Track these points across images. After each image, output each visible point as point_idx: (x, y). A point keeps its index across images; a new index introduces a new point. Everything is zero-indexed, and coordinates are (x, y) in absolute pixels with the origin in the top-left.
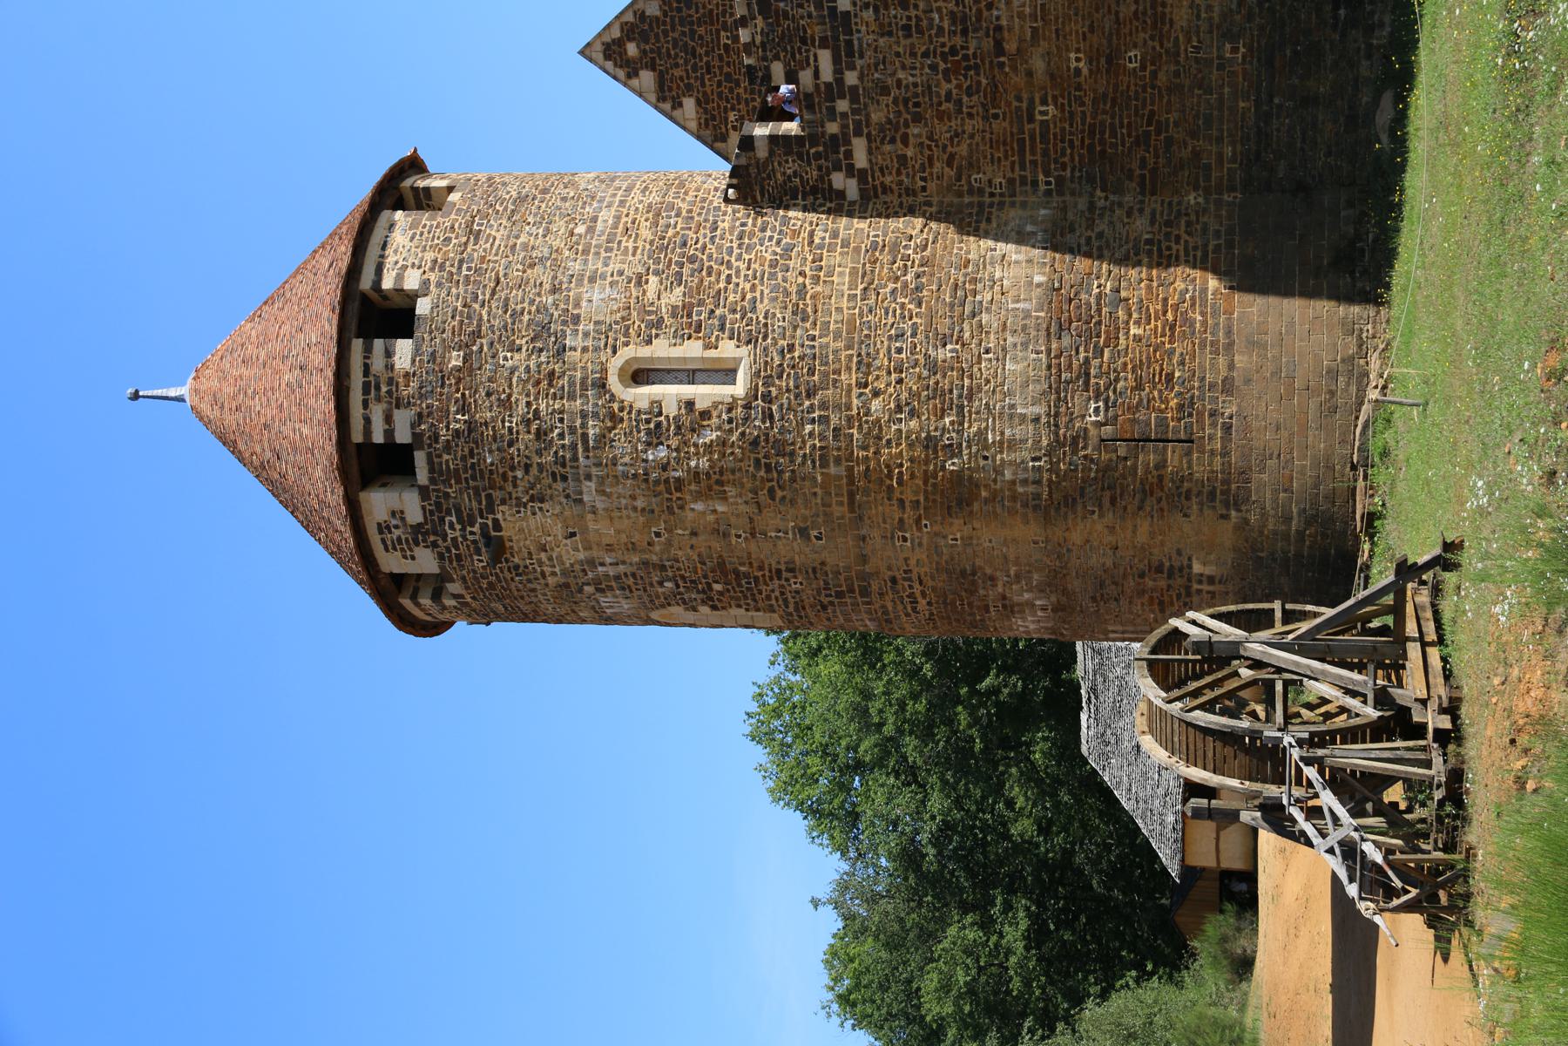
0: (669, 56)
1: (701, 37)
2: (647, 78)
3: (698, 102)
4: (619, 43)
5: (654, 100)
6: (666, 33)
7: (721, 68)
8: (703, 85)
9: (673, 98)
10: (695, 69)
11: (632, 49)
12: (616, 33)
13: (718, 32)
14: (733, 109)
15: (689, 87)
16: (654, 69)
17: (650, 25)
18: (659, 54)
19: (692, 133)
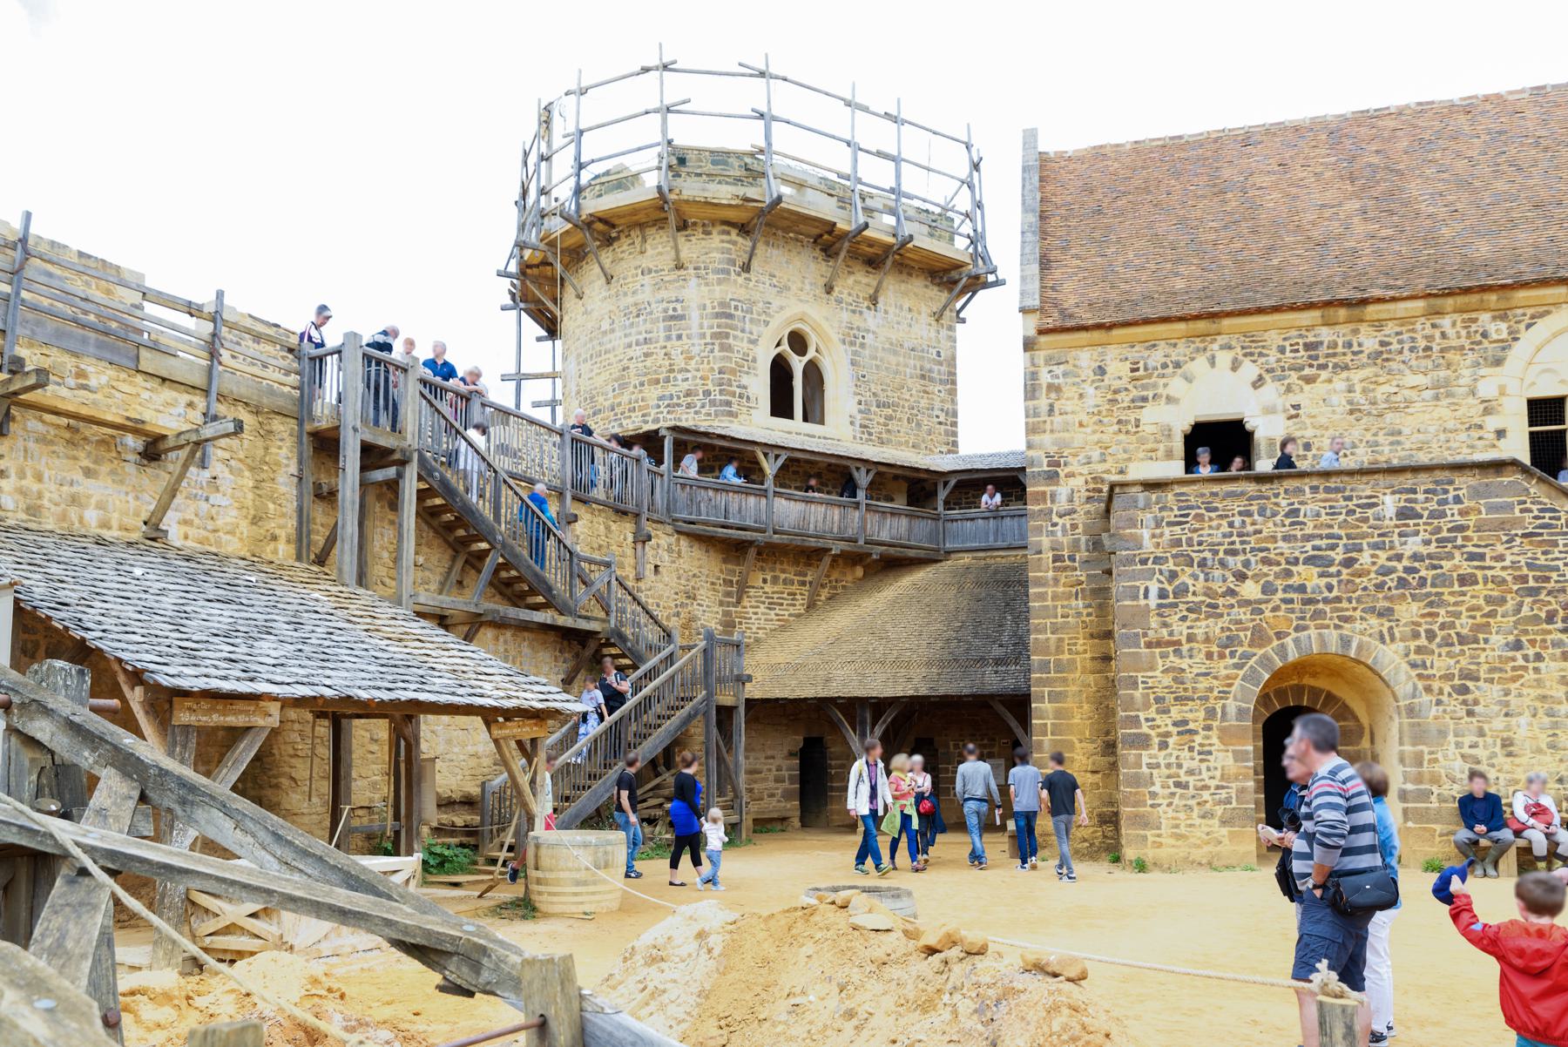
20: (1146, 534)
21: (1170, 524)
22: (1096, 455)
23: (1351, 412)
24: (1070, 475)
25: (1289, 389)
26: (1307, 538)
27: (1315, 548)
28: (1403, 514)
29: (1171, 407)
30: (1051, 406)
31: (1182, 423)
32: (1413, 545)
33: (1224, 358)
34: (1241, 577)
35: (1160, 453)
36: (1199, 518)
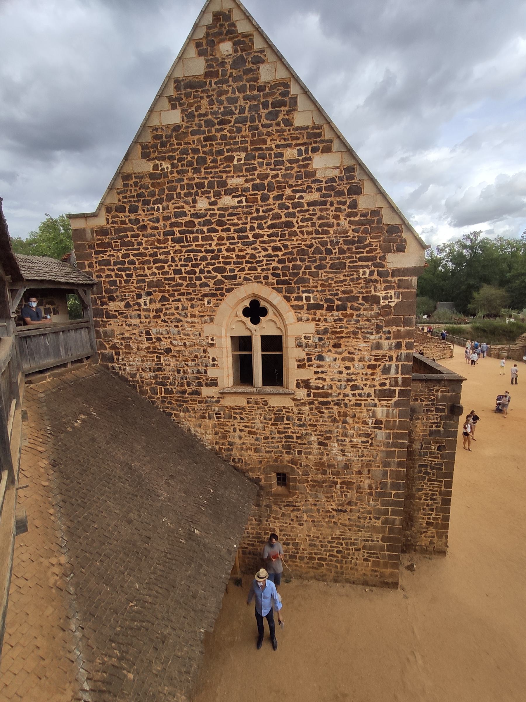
0: (220, 94)
1: (239, 130)
2: (197, 67)
3: (177, 128)
4: (231, 33)
5: (179, 74)
6: (242, 90)
7: (210, 153)
8: (193, 133)
9: (179, 99)
10: (209, 123)
11: (226, 48)
12: (242, 27)
13: (245, 150)
14: (173, 166)
15: (190, 116)
16: (207, 75)
17: (250, 70)
18: (222, 82)
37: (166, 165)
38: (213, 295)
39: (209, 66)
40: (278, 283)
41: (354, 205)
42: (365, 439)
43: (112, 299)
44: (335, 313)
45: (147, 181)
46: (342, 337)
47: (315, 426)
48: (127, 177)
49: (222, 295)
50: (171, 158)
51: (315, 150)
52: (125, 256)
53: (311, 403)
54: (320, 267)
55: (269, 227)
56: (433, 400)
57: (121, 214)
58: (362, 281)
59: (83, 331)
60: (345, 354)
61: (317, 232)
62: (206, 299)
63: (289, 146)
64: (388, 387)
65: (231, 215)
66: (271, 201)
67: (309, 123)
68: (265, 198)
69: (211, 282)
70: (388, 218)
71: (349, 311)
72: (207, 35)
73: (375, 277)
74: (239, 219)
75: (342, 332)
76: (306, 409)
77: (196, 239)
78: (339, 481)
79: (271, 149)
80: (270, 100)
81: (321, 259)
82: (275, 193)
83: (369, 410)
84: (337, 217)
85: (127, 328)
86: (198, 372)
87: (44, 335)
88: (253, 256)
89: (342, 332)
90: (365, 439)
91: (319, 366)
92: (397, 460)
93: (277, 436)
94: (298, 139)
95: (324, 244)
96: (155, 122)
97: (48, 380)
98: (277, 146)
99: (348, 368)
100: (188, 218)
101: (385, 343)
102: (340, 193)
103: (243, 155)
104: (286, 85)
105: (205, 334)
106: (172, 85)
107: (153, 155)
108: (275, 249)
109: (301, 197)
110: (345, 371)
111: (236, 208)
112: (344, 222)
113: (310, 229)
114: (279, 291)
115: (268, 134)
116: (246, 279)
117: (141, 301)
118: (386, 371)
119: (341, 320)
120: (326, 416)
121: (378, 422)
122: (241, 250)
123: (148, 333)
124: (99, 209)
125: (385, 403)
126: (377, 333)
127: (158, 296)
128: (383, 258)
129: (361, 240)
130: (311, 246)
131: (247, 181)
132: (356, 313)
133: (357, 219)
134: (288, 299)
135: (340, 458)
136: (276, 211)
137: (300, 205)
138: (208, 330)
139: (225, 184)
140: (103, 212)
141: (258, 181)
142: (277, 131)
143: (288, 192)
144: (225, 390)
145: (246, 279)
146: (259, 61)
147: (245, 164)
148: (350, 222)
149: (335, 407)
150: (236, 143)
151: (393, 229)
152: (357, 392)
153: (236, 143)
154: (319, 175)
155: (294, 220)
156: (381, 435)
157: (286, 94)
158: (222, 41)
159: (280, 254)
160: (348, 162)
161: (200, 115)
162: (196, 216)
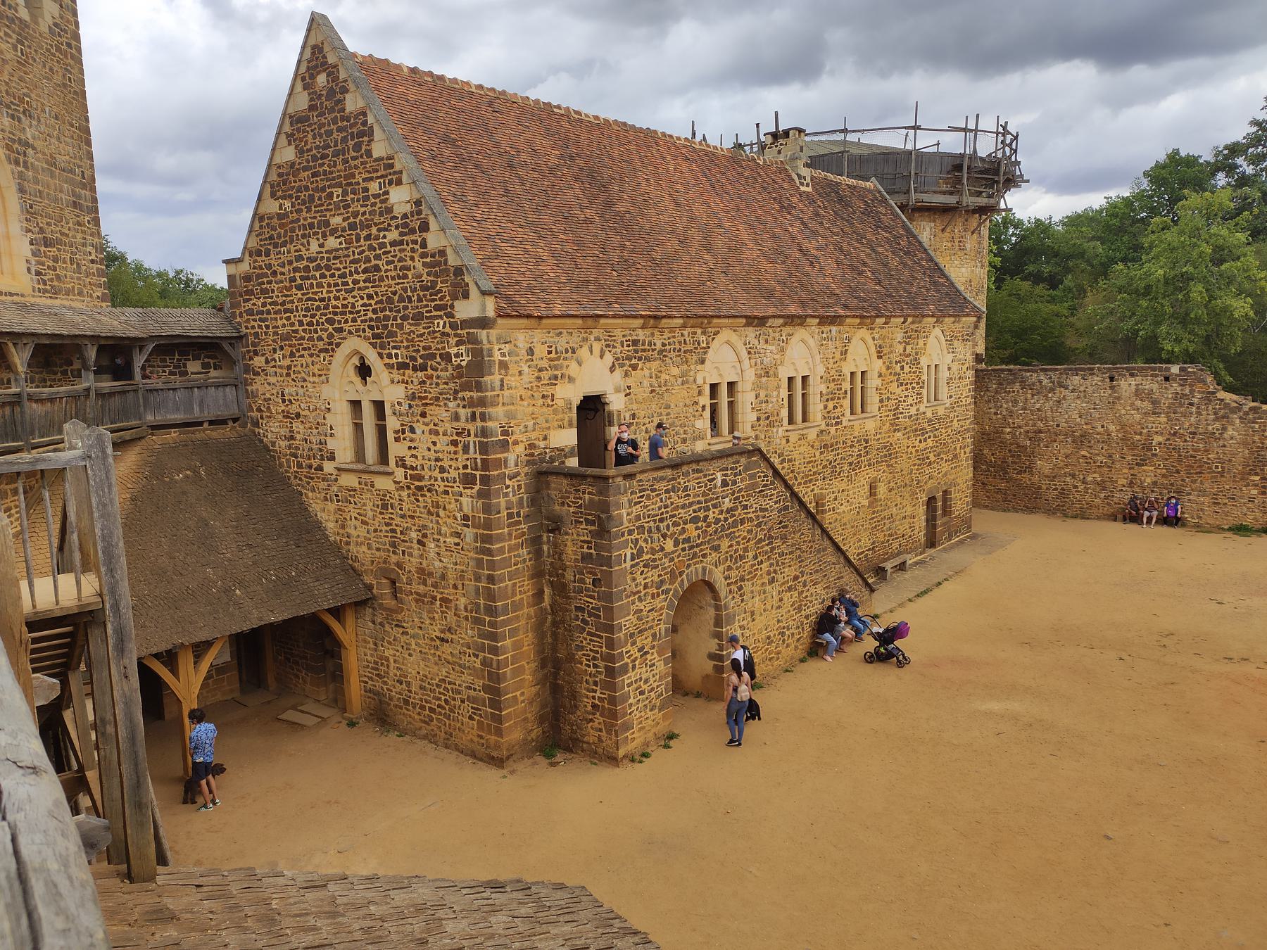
3: (292, 164)
6: (335, 121)
10: (315, 159)
11: (322, 79)
12: (331, 59)
16: (312, 108)
17: (339, 101)
19: (271, 159)
20: (624, 512)
21: (636, 504)
22: (530, 424)
23: (653, 391)
24: (516, 443)
25: (626, 375)
26: (691, 504)
27: (694, 511)
28: (724, 483)
29: (569, 386)
30: (502, 381)
31: (576, 401)
32: (727, 504)
33: (597, 347)
34: (664, 536)
35: (566, 423)
36: (648, 497)
37: (287, 204)
38: (326, 351)
39: (312, 100)
40: (375, 336)
41: (424, 245)
42: (457, 540)
43: (256, 353)
44: (419, 374)
45: (275, 222)
46: (426, 404)
47: (413, 517)
48: (261, 219)
49: (333, 350)
50: (290, 196)
51: (390, 183)
52: (264, 305)
53: (409, 488)
54: (404, 318)
55: (365, 271)
56: (580, 507)
57: (259, 259)
58: (438, 335)
59: (228, 389)
60: (431, 426)
61: (399, 278)
62: (322, 355)
63: (371, 179)
64: (469, 471)
65: (335, 258)
66: (362, 242)
67: (384, 154)
68: (358, 240)
69: (325, 336)
70: (453, 260)
71: (430, 372)
72: (308, 69)
73: (448, 330)
74: (341, 262)
75: (426, 398)
76: (404, 493)
77: (312, 286)
78: (439, 596)
79: (358, 183)
80: (355, 130)
81: (405, 308)
82: (364, 234)
83: (457, 501)
84: (412, 259)
85: (268, 388)
86: (321, 443)
87: (174, 389)
88: (353, 306)
89: (426, 398)
90: (457, 540)
91: (412, 440)
92: (486, 572)
93: (385, 528)
94: (377, 171)
95: (405, 290)
96: (277, 160)
97: (173, 435)
98: (364, 180)
99: (434, 444)
100: (305, 263)
101: (463, 413)
102: (413, 231)
103: (340, 190)
104: (365, 114)
105: (323, 397)
106: (287, 121)
107: (279, 194)
108: (370, 297)
109: (385, 237)
110: (433, 448)
111: (337, 250)
112: (419, 265)
113: (393, 273)
114: (374, 345)
115: (356, 167)
116: (350, 332)
117: (276, 356)
118: (466, 449)
119: (424, 382)
120: (422, 505)
121: (466, 518)
122: (345, 299)
123: (283, 395)
124: (243, 254)
125: (469, 492)
126: (455, 399)
127: (287, 351)
128: (452, 306)
129: (434, 284)
130: (395, 293)
131: (344, 220)
132: (435, 374)
133: (428, 260)
134: (380, 355)
135: (437, 564)
136: (367, 253)
137: (382, 246)
138: (326, 391)
139: (327, 223)
140: (247, 257)
141: (352, 220)
142: (362, 163)
143: (374, 230)
144: (343, 466)
145: (350, 332)
146: (345, 91)
147: (342, 201)
148: (424, 264)
149: (428, 494)
150: (333, 179)
151: (459, 271)
152: (445, 475)
153: (333, 179)
154: (398, 211)
155: (380, 263)
156: (469, 533)
157: (365, 123)
158: (318, 73)
159: (373, 302)
160: (416, 196)
161: (308, 151)
162: (310, 259)
